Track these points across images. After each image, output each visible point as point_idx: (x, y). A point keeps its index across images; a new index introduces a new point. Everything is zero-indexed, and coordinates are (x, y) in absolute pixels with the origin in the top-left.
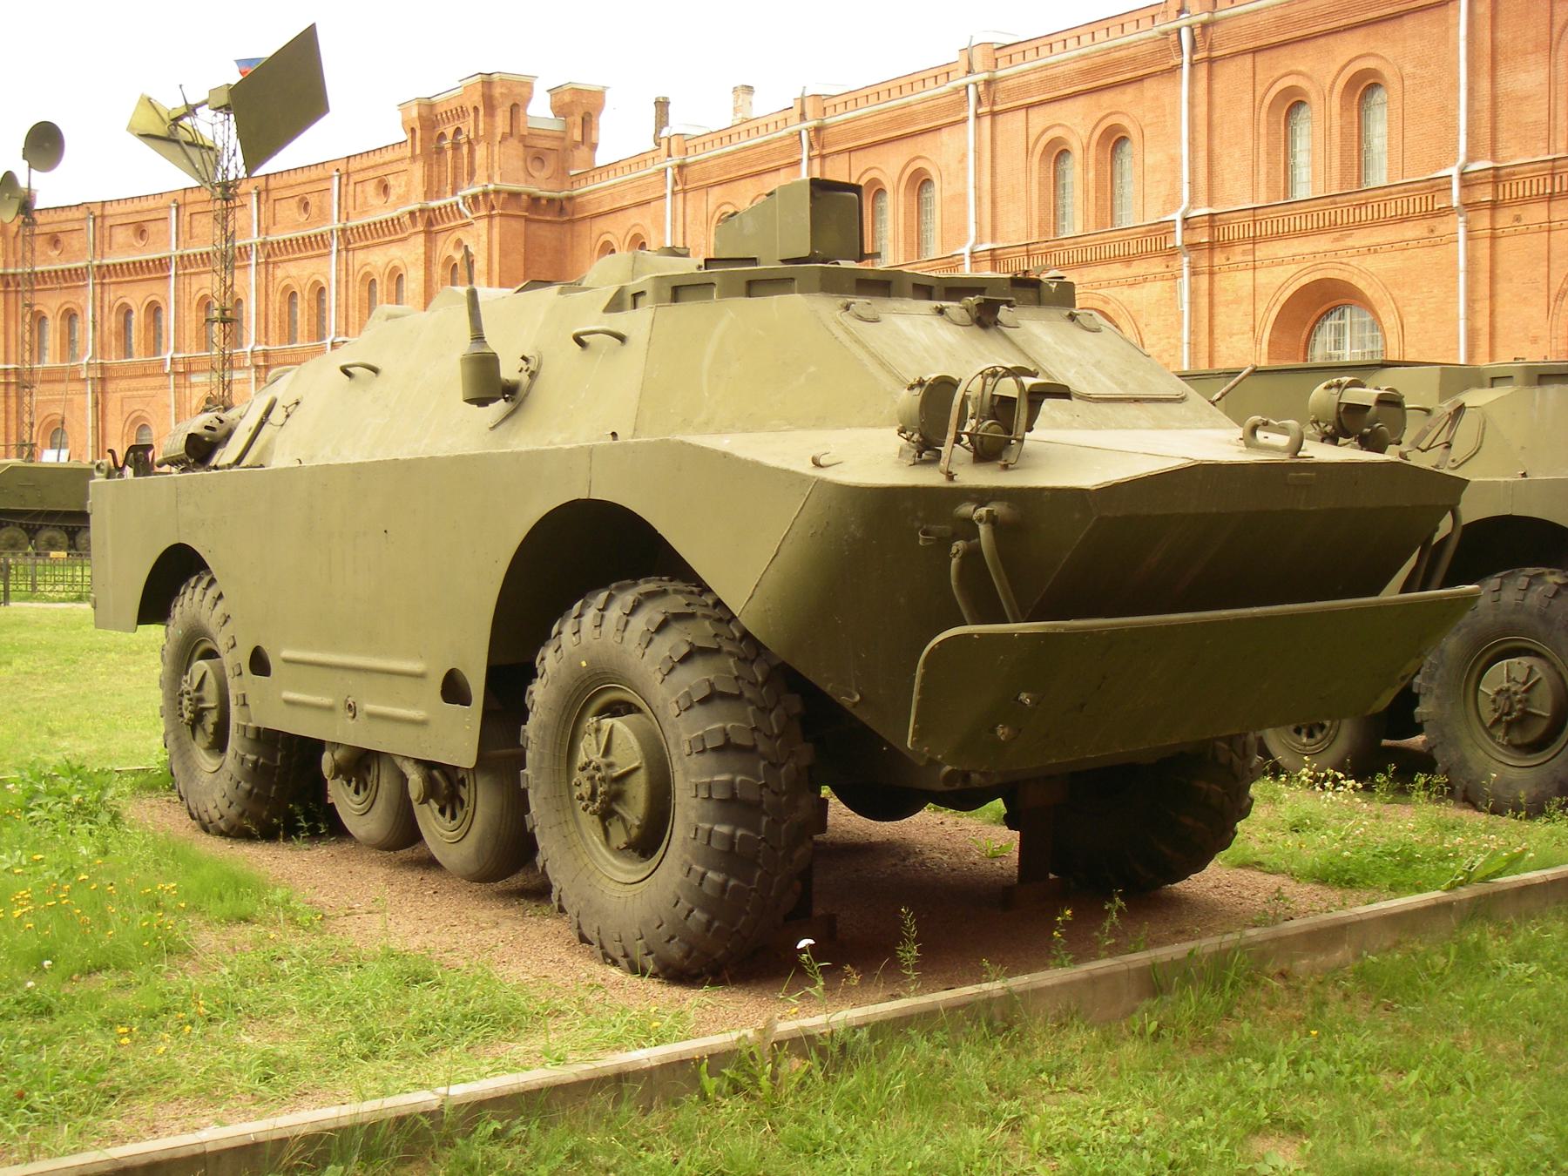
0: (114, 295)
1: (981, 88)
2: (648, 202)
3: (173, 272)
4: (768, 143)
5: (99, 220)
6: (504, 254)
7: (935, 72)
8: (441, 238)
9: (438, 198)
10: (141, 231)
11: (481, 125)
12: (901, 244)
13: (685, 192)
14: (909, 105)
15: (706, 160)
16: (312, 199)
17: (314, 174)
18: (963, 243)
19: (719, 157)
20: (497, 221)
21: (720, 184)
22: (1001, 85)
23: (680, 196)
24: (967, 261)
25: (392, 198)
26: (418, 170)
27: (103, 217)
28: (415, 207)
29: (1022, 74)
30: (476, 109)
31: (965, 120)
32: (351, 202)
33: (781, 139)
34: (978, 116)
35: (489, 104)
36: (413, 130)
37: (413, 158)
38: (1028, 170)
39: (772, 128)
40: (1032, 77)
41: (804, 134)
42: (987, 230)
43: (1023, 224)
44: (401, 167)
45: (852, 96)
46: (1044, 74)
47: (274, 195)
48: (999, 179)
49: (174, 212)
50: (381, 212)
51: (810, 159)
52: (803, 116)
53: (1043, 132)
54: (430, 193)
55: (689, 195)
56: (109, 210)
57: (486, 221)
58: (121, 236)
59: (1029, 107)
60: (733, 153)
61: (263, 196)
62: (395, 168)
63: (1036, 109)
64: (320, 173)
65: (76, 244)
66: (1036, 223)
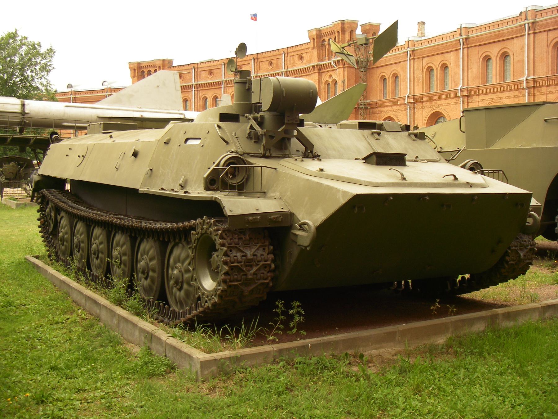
0: (201, 94)
1: (530, 25)
2: (400, 62)
3: (223, 86)
4: (447, 43)
5: (196, 69)
6: (349, 79)
7: (512, 19)
8: (324, 75)
9: (322, 61)
10: (211, 72)
11: (340, 37)
12: (498, 77)
13: (414, 59)
14: (502, 30)
15: (422, 49)
16: (274, 62)
17: (275, 53)
18: (523, 76)
19: (427, 47)
20: (346, 69)
21: (428, 56)
22: (537, 24)
23: (412, 61)
24: (525, 82)
25: (305, 61)
26: (315, 52)
27: (198, 68)
28: (315, 64)
29: (547, 20)
30: (338, 32)
31: (525, 35)
32: (289, 63)
33: (452, 42)
34: (529, 34)
35: (343, 30)
36: (314, 39)
37: (314, 48)
38: (547, 52)
39: (448, 38)
40: (550, 21)
41: (461, 40)
42: (532, 72)
43: (545, 70)
44: (308, 51)
45: (480, 27)
46: (555, 20)
47: (259, 60)
48: (536, 55)
49: (223, 66)
50: (300, 66)
51: (463, 48)
52: (461, 35)
53: (554, 39)
54: (319, 60)
55: (415, 60)
56: (200, 66)
57: (342, 69)
58: (204, 74)
59: (548, 31)
60: (433, 46)
61: (256, 61)
62: (305, 51)
63: (551, 32)
64: (277, 53)
65: (188, 77)
66: (550, 69)
